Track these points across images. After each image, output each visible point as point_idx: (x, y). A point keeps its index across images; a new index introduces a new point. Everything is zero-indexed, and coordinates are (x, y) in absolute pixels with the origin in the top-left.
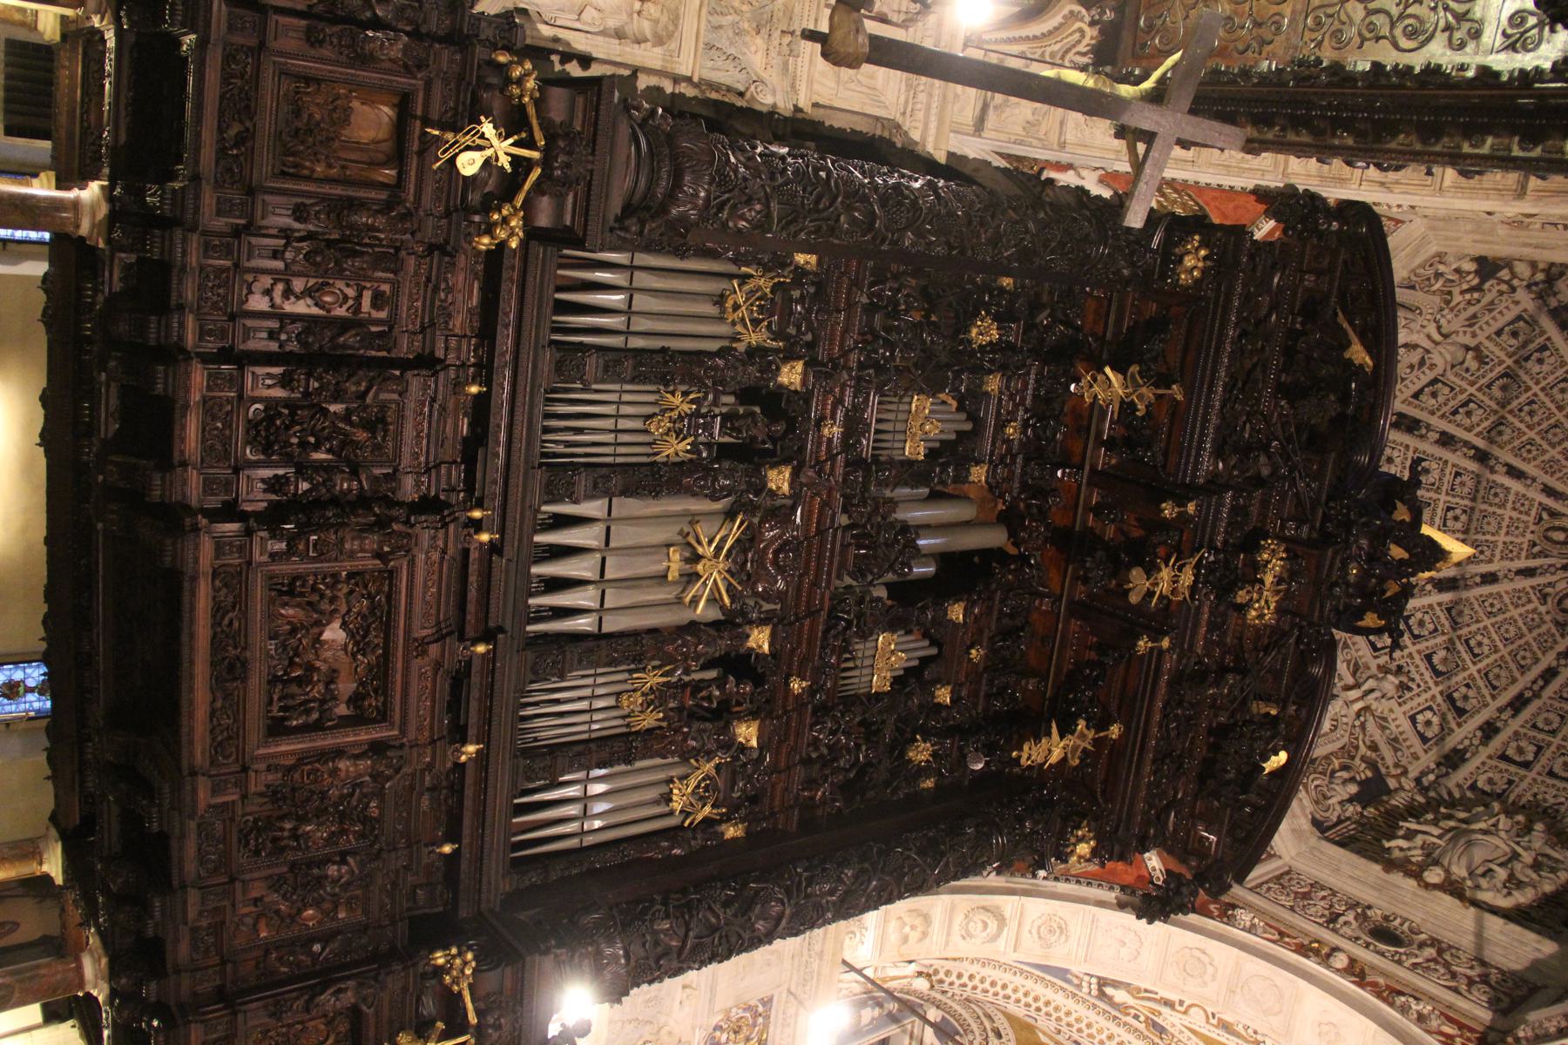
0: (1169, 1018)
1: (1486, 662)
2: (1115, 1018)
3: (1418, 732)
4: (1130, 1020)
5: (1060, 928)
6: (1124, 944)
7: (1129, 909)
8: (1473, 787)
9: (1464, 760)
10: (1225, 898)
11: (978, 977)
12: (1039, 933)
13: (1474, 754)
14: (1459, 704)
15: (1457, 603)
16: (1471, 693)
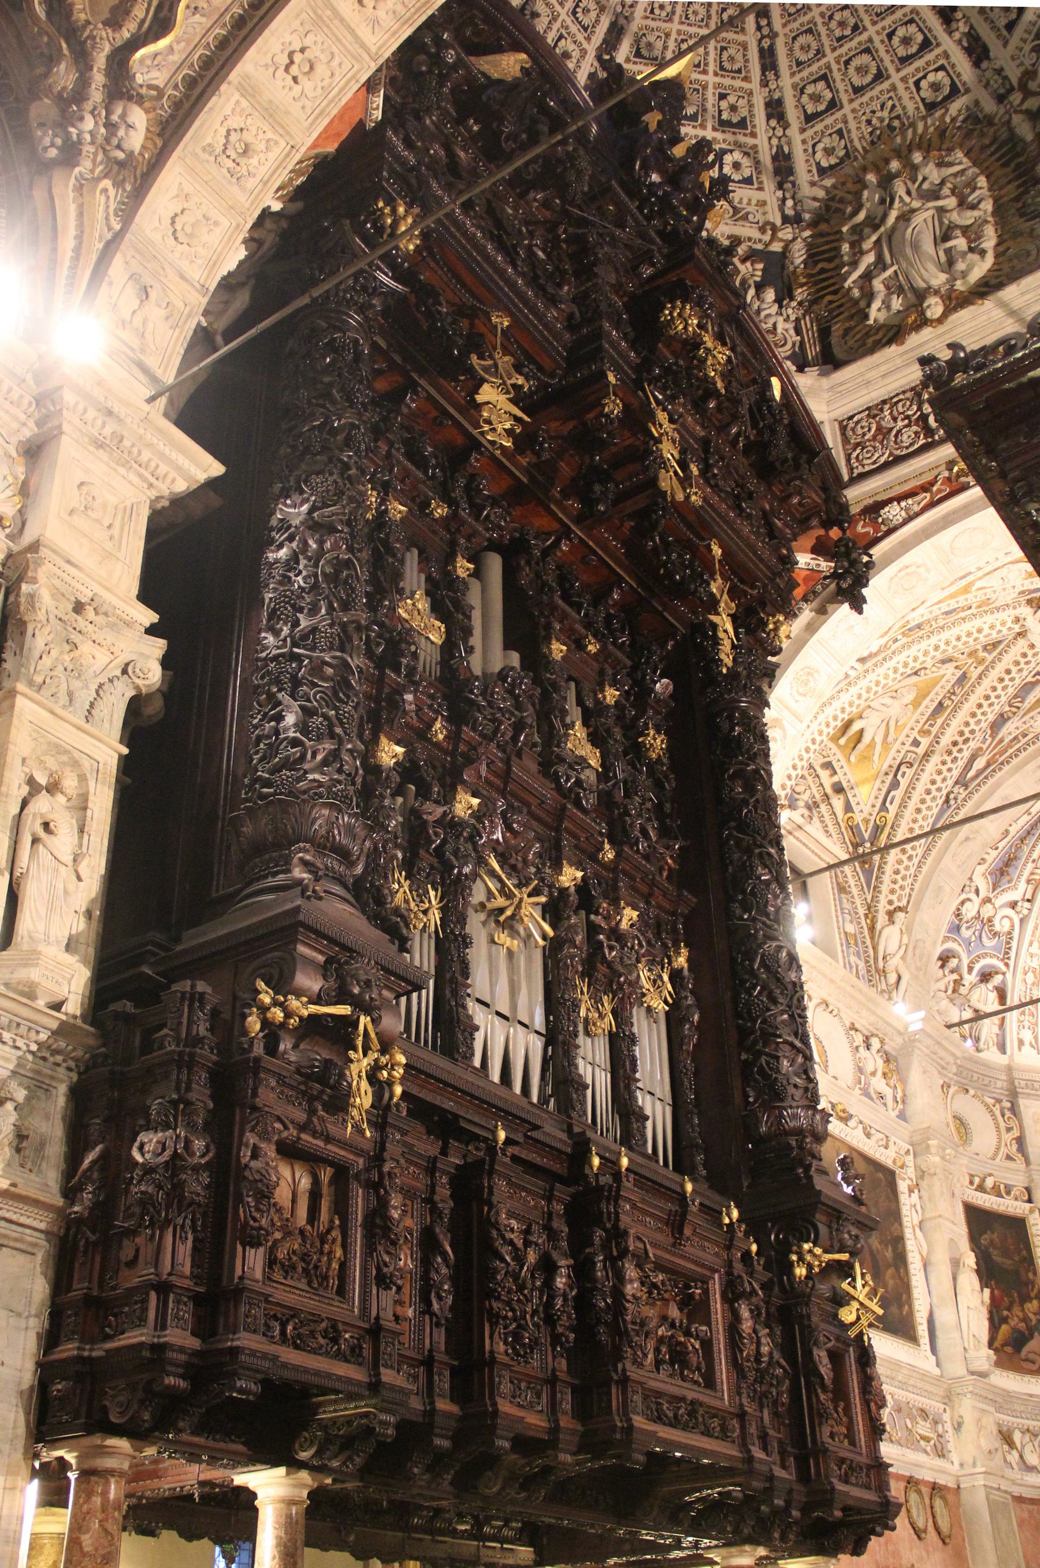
0: (915, 618)
1: (711, 59)
2: (884, 659)
3: (739, 182)
4: (894, 647)
5: (809, 674)
6: (852, 627)
7: (830, 607)
8: (822, 171)
9: (788, 157)
10: (854, 510)
11: (797, 761)
12: (801, 694)
13: (789, 144)
14: (735, 120)
15: (637, 41)
16: (732, 99)
